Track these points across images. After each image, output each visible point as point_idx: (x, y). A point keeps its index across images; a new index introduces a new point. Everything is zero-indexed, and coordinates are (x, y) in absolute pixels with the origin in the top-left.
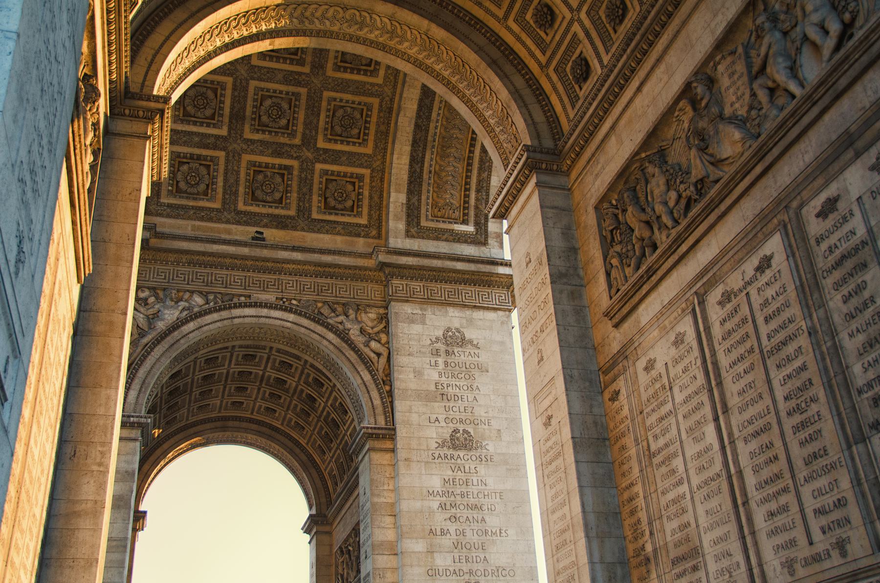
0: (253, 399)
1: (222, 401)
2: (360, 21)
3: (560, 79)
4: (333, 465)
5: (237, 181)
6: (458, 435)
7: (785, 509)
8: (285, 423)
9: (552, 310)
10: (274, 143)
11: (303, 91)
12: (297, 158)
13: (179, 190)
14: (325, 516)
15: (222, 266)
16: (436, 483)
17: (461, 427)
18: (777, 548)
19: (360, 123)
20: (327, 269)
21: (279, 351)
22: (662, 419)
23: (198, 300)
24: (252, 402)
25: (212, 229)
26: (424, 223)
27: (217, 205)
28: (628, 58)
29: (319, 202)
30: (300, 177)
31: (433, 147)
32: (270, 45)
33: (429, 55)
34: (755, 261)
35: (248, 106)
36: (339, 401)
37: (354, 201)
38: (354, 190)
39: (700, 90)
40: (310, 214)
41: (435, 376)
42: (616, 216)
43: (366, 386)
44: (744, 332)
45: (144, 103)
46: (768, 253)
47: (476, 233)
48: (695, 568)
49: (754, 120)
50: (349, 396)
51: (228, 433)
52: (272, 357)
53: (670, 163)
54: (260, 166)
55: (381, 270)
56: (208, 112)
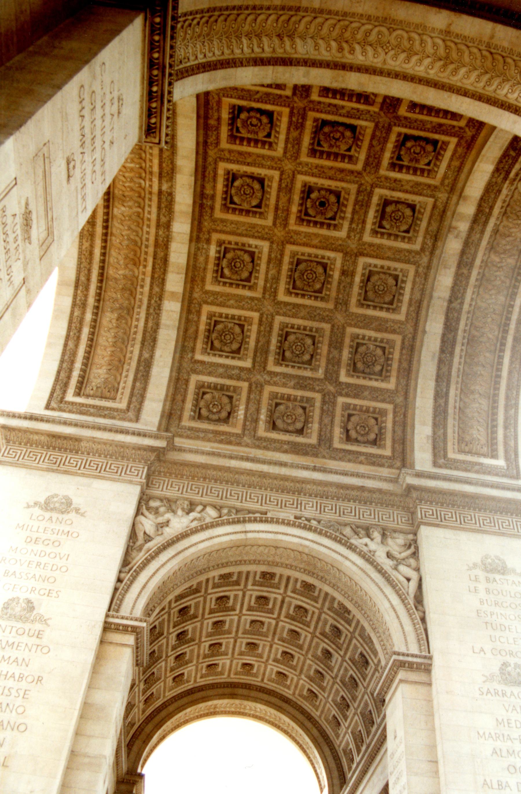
0: (264, 660)
1: (232, 661)
2: (408, 46)
6: (509, 669)
8: (297, 692)
10: (297, 376)
11: (327, 327)
17: (512, 661)
23: (211, 513)
24: (263, 665)
26: (451, 455)
36: (359, 651)
37: (377, 435)
38: (377, 424)
52: (287, 599)
55: (407, 496)
56: (235, 346)
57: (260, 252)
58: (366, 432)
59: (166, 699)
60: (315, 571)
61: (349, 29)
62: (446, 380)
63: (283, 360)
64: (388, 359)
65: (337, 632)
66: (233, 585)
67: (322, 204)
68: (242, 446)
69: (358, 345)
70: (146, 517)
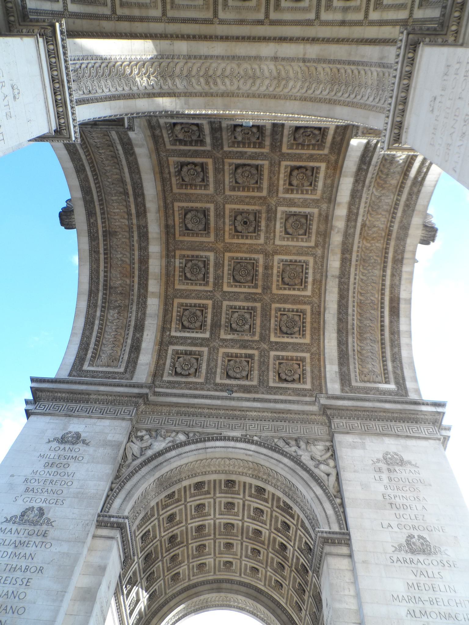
0: (238, 557)
1: (215, 560)
6: (414, 540)
11: (258, 305)
12: (257, 349)
15: (201, 415)
17: (416, 533)
20: (281, 415)
24: (239, 561)
26: (354, 384)
27: (201, 380)
30: (260, 362)
35: (222, 318)
37: (300, 375)
47: (398, 390)
51: (222, 594)
52: (247, 503)
57: (208, 260)
58: (292, 374)
59: (167, 596)
60: (260, 475)
62: (345, 333)
64: (303, 323)
65: (287, 527)
66: (205, 494)
67: (245, 223)
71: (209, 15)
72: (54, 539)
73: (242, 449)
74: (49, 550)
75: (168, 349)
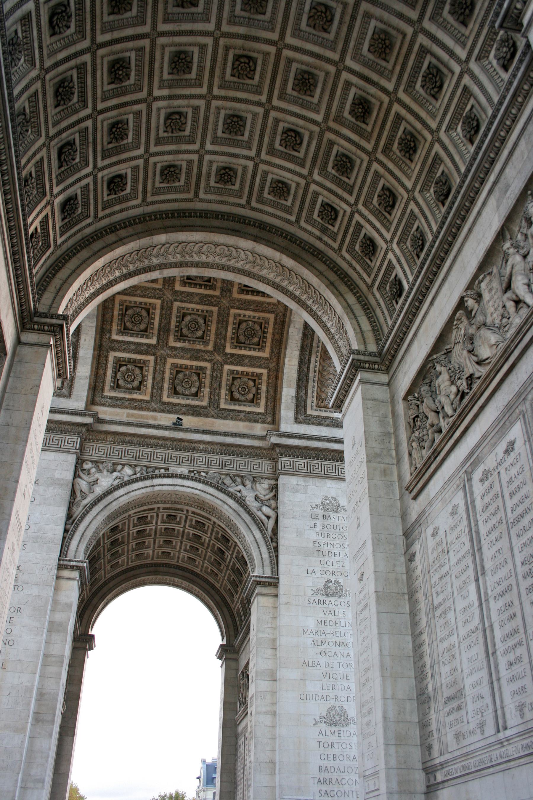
0: (178, 550)
1: (153, 552)
3: (382, 296)
4: (239, 605)
5: (163, 379)
6: (331, 584)
7: (519, 659)
9: (366, 485)
11: (215, 309)
12: (209, 361)
13: (118, 386)
14: (233, 646)
15: (147, 445)
16: (310, 623)
17: (333, 578)
18: (515, 693)
19: (260, 333)
21: (193, 513)
22: (442, 578)
23: (128, 471)
25: (142, 416)
26: (309, 412)
27: (147, 398)
28: (423, 279)
29: (226, 395)
31: (317, 351)
32: (160, 274)
33: (283, 279)
34: (503, 446)
35: (172, 321)
39: (470, 303)
40: (219, 405)
41: (314, 536)
42: (418, 406)
43: (257, 542)
44: (496, 506)
45: (48, 320)
46: (512, 439)
48: (459, 708)
49: (505, 327)
50: (245, 550)
51: (159, 577)
52: (189, 517)
53: (452, 363)
54: (181, 367)
56: (143, 326)
61: (188, 247)
63: (181, 336)
68: (151, 411)
69: (240, 323)
70: (81, 478)
71: (191, 195)
72: (24, 582)
73: (189, 487)
74: (22, 593)
75: (108, 355)
